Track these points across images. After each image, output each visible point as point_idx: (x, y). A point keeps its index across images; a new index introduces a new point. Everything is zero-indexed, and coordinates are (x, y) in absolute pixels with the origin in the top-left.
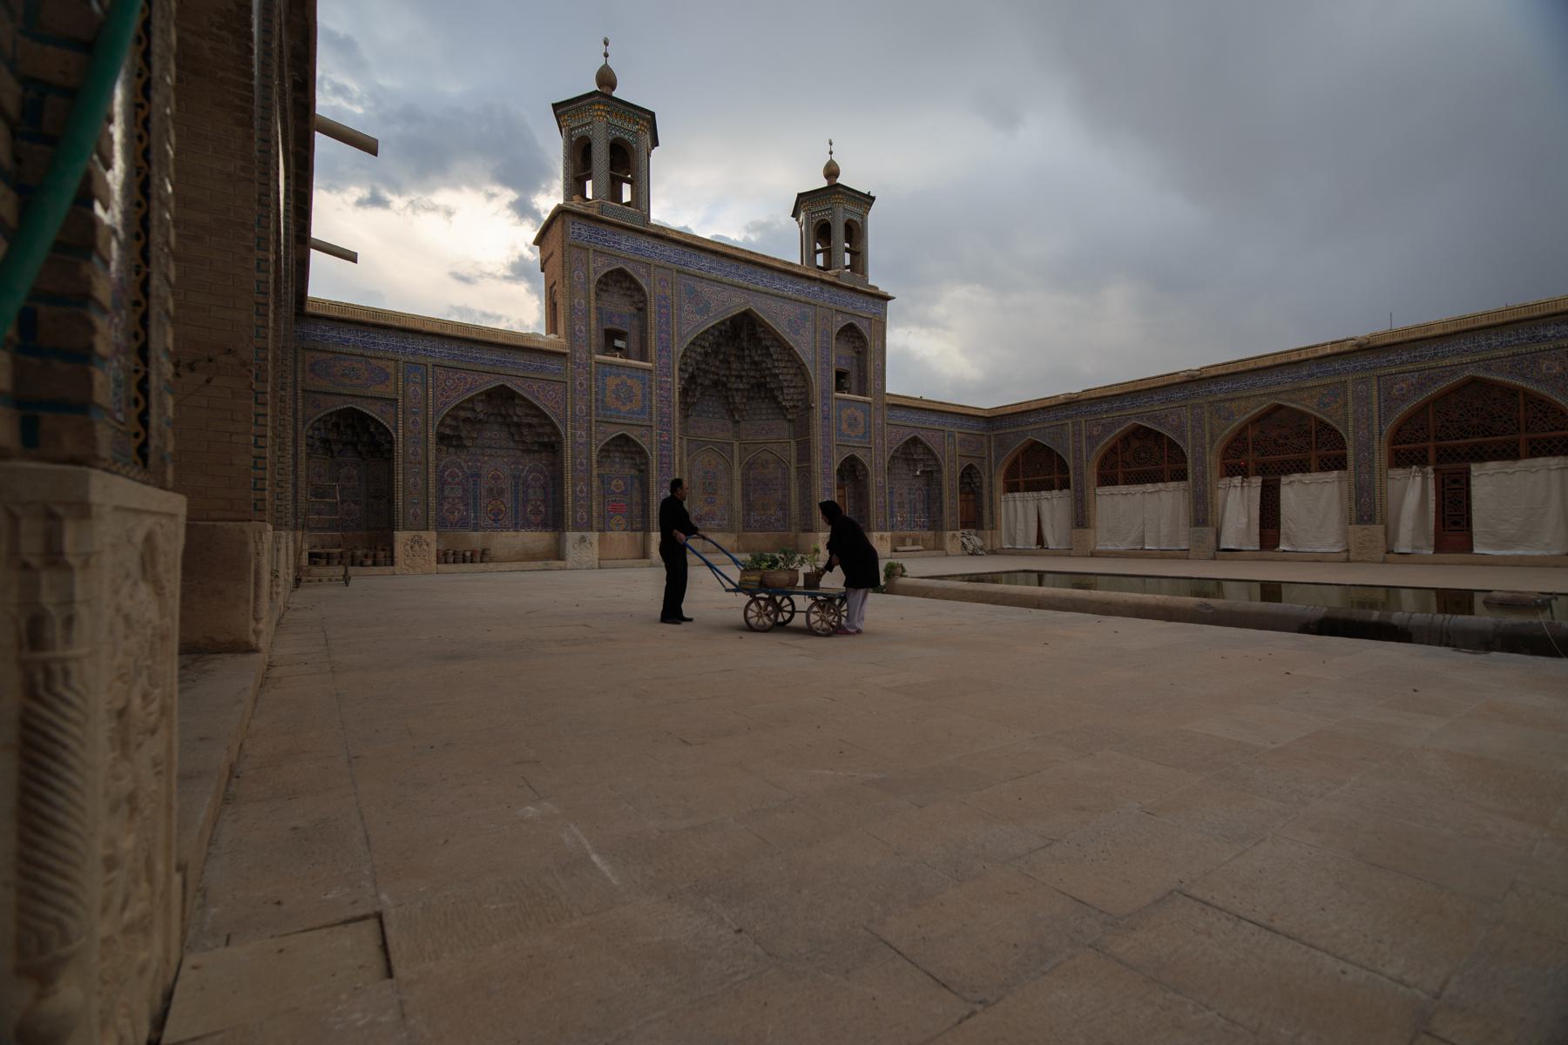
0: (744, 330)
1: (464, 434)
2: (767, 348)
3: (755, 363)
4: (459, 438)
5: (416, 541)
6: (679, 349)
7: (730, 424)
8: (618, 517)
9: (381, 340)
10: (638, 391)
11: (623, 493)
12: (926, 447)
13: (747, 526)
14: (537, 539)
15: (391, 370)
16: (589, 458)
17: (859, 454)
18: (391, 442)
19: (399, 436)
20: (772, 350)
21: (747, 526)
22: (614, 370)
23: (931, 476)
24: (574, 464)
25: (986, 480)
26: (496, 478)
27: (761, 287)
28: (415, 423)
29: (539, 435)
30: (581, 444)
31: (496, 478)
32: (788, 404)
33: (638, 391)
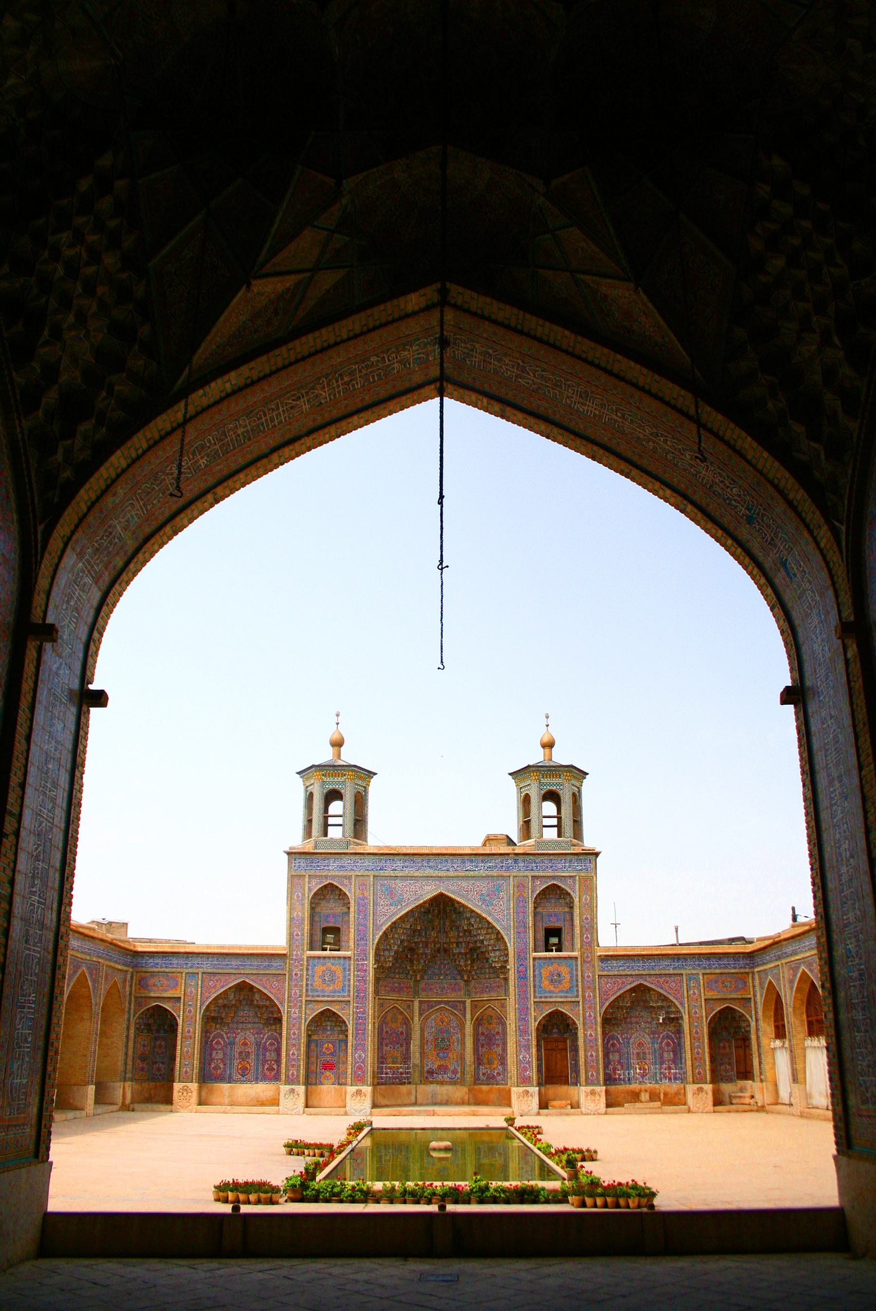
0: (441, 908)
1: (223, 1015)
2: (468, 919)
3: (465, 931)
4: (222, 1019)
5: (186, 1090)
6: (374, 938)
7: (462, 983)
8: (328, 1073)
9: (175, 961)
11: (332, 1054)
12: (660, 994)
14: (262, 1089)
16: (300, 1029)
18: (177, 1025)
19: (180, 1022)
20: (472, 920)
21: (477, 1080)
22: (321, 960)
23: (674, 1021)
24: (288, 1034)
25: (753, 1024)
26: (245, 1044)
27: (451, 874)
28: (190, 1011)
29: (272, 1012)
30: (296, 1018)
31: (245, 1044)
32: (498, 965)
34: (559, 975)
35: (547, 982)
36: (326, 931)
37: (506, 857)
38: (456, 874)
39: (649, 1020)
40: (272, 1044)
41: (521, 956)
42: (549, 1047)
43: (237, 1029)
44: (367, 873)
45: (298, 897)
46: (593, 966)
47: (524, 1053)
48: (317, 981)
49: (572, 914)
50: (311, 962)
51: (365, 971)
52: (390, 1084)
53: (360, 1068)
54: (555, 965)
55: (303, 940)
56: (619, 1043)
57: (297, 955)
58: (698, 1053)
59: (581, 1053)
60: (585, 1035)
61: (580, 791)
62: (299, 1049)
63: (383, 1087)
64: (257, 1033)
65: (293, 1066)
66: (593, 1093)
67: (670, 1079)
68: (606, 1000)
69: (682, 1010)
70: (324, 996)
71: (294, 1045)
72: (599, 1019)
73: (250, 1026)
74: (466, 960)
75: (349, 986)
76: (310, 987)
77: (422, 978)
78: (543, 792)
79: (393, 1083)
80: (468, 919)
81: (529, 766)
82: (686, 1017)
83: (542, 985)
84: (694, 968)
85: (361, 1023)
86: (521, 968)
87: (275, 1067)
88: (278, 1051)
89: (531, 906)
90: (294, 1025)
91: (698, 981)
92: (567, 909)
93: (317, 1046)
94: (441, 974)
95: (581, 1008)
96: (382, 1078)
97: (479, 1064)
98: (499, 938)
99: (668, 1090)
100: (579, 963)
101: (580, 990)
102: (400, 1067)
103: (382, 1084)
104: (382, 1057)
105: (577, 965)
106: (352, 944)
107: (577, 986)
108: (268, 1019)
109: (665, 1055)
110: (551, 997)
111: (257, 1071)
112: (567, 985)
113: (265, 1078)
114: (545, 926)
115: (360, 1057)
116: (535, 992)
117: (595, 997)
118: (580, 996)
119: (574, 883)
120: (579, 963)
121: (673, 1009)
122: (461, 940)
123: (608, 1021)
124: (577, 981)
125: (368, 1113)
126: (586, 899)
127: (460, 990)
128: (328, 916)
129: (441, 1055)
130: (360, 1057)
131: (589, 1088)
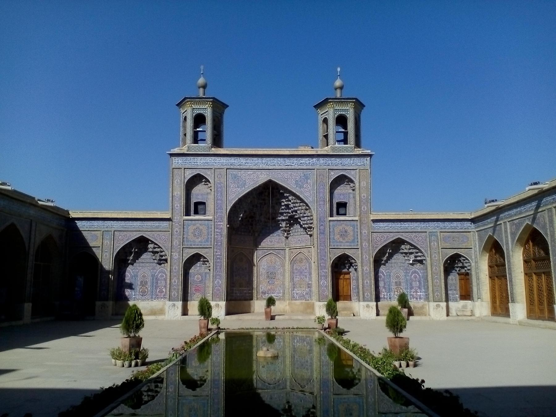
2: (287, 197)
3: (285, 205)
8: (198, 294)
10: (205, 231)
11: (200, 281)
13: (293, 298)
15: (99, 235)
16: (179, 266)
17: (349, 253)
20: (290, 198)
25: (473, 264)
26: (144, 276)
27: (277, 167)
29: (162, 256)
31: (144, 276)
33: (205, 231)
35: (338, 236)
36: (197, 204)
38: (280, 167)
39: (404, 261)
40: (162, 276)
41: (321, 220)
43: (139, 266)
44: (222, 167)
45: (177, 182)
46: (368, 226)
48: (191, 236)
49: (354, 194)
50: (186, 222)
51: (222, 228)
53: (219, 290)
54: (343, 225)
55: (181, 209)
56: (384, 275)
57: (177, 219)
58: (437, 283)
59: (360, 281)
60: (363, 270)
61: (359, 117)
62: (178, 279)
64: (152, 269)
65: (175, 289)
66: (368, 306)
67: (417, 299)
68: (376, 247)
69: (426, 255)
70: (194, 245)
71: (175, 276)
72: (372, 260)
73: (147, 265)
74: (287, 224)
75: (211, 238)
76: (185, 239)
77: (259, 235)
78: (336, 116)
79: (240, 300)
80: (287, 197)
82: (428, 259)
83: (336, 238)
84: (434, 228)
85: (218, 262)
86: (322, 227)
87: (164, 290)
88: (165, 280)
90: (175, 264)
91: (437, 236)
95: (360, 252)
97: (294, 288)
98: (308, 207)
99: (416, 305)
105: (357, 225)
106: (213, 212)
107: (358, 238)
108: (160, 260)
109: (414, 283)
110: (340, 246)
111: (152, 292)
112: (352, 238)
113: (157, 298)
115: (218, 282)
117: (369, 246)
120: (359, 224)
121: (420, 254)
123: (378, 262)
124: (357, 235)
126: (364, 184)
128: (198, 195)
129: (270, 282)
130: (218, 282)
131: (365, 303)
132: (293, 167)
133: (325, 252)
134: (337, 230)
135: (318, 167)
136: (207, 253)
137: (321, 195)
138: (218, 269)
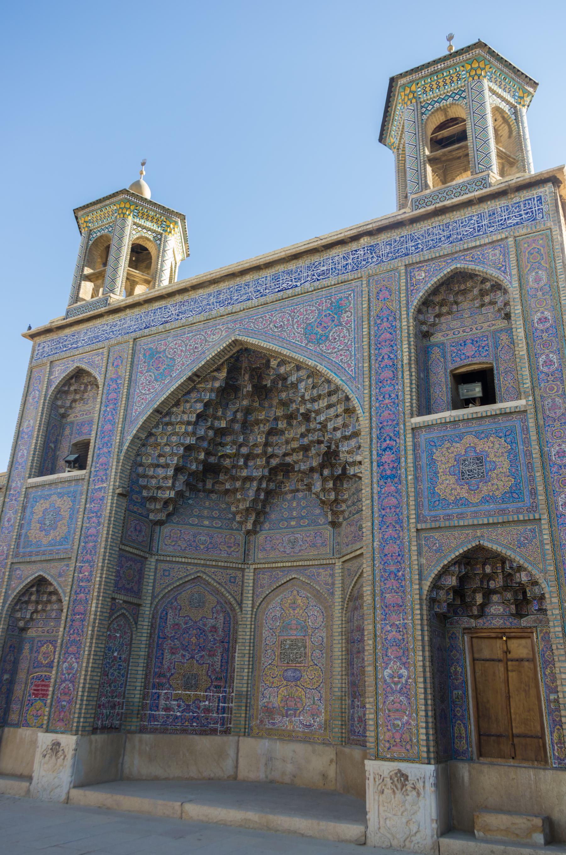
7: (328, 531)
17: (497, 542)
34: (480, 460)
37: (354, 246)
38: (262, 300)
42: (486, 654)
47: (394, 665)
52: (175, 732)
54: (469, 439)
63: (147, 737)
70: (38, 553)
74: (324, 480)
76: (22, 540)
79: (184, 731)
81: (393, 81)
86: (388, 457)
89: (406, 324)
92: (501, 324)
93: (31, 650)
94: (293, 518)
96: (154, 718)
100: (531, 423)
101: (540, 488)
102: (208, 699)
103: (154, 731)
104: (160, 675)
110: (461, 516)
114: (451, 367)
115: (70, 668)
116: (418, 506)
118: (542, 506)
119: (505, 254)
120: (531, 423)
122: (306, 441)
125: (64, 796)
126: (537, 280)
127: (324, 545)
130: (70, 668)
132: (298, 290)
133: (401, 548)
134: (445, 458)
135: (372, 268)
136: (60, 575)
137: (385, 350)
138: (77, 624)
